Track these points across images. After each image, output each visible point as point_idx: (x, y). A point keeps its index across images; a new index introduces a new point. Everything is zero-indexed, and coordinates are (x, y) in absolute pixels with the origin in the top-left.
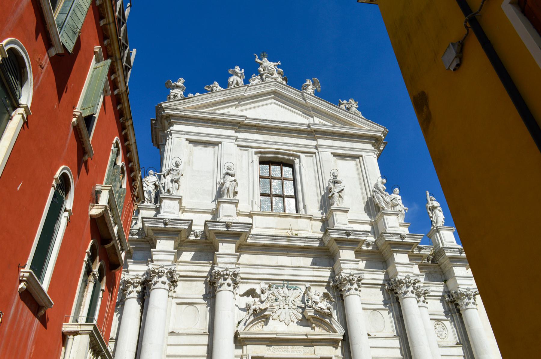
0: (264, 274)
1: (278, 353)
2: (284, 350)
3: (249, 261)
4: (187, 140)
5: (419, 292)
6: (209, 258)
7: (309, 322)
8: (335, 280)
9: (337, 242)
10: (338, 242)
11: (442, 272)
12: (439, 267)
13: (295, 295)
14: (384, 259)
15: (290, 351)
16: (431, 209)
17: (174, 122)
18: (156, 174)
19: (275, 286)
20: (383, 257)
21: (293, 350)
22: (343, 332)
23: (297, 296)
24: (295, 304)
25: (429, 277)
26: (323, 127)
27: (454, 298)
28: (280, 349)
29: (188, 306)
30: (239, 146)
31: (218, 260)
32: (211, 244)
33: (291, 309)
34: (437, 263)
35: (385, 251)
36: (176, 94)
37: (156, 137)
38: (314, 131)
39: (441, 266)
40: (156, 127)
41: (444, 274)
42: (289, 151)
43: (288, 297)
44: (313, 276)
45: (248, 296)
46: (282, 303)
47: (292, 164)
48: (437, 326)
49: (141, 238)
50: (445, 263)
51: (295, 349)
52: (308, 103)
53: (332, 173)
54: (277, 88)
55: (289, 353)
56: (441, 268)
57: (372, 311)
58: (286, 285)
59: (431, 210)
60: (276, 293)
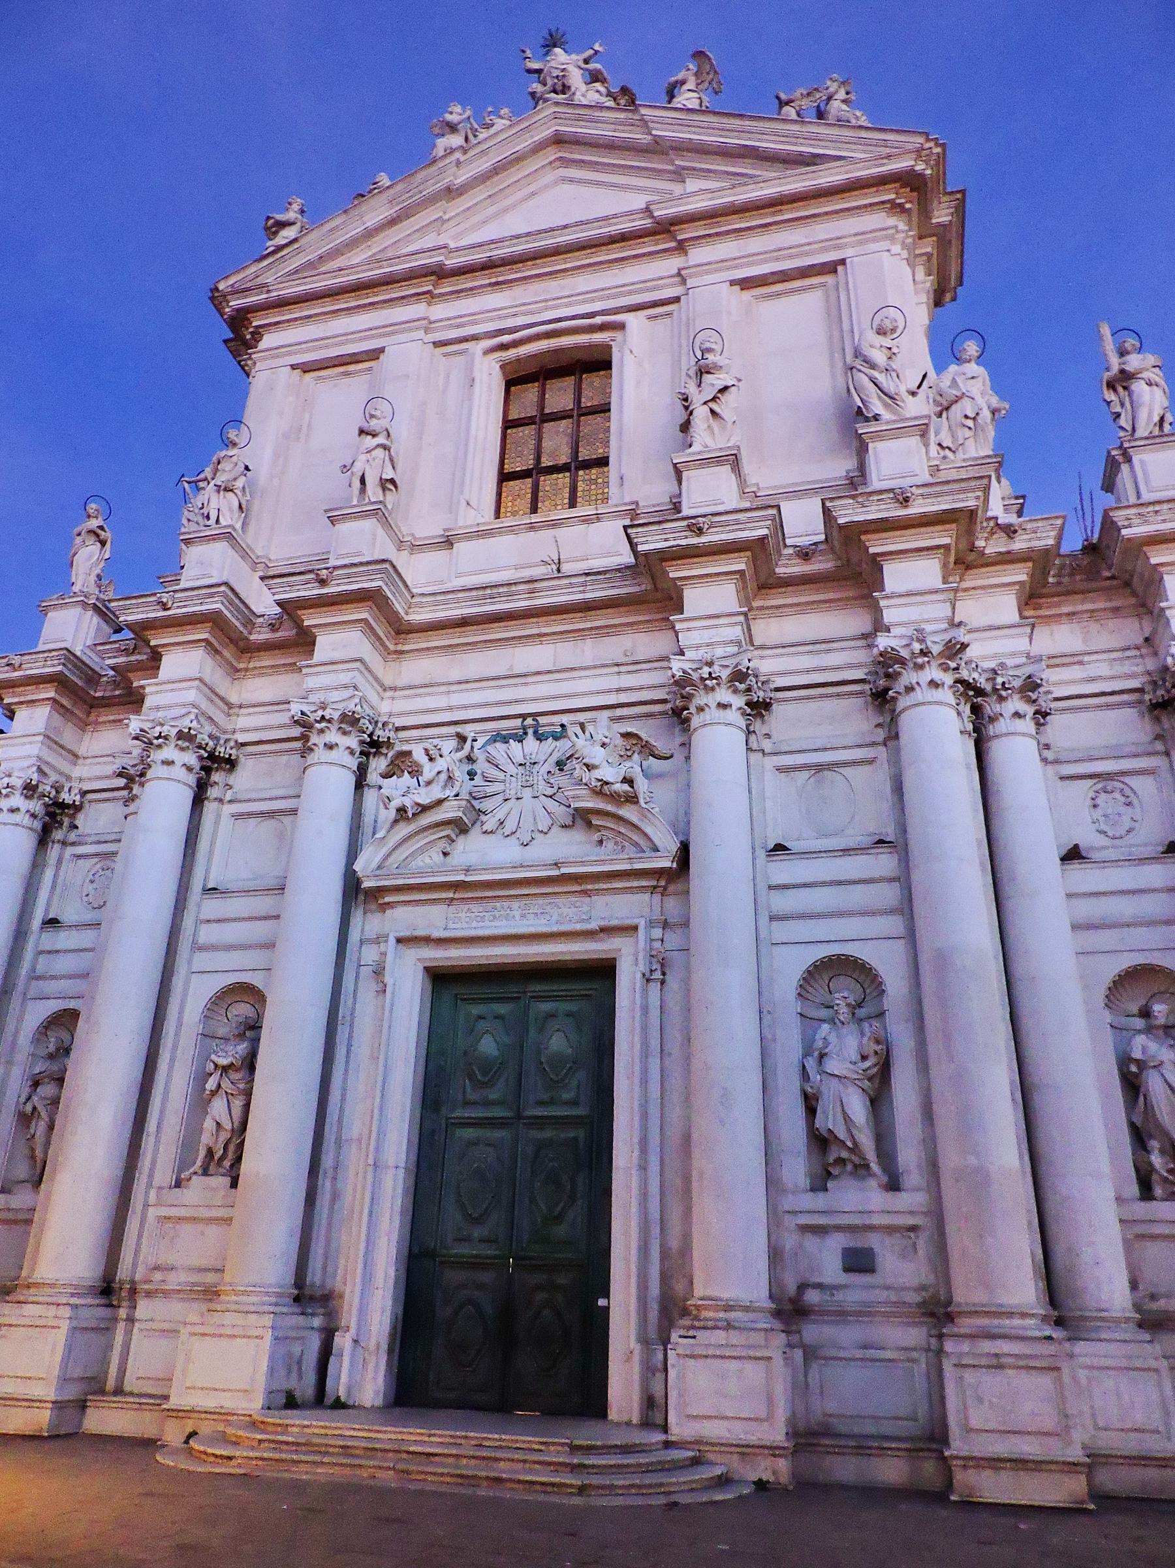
0: (465, 707)
1: (481, 924)
2: (496, 913)
5: (999, 687)
15: (517, 917)
21: (527, 912)
24: (552, 781)
26: (697, 202)
30: (438, 344)
34: (1113, 578)
43: (535, 763)
44: (619, 690)
47: (606, 358)
48: (1102, 799)
54: (560, 125)
55: (512, 923)
57: (813, 772)
58: (530, 731)
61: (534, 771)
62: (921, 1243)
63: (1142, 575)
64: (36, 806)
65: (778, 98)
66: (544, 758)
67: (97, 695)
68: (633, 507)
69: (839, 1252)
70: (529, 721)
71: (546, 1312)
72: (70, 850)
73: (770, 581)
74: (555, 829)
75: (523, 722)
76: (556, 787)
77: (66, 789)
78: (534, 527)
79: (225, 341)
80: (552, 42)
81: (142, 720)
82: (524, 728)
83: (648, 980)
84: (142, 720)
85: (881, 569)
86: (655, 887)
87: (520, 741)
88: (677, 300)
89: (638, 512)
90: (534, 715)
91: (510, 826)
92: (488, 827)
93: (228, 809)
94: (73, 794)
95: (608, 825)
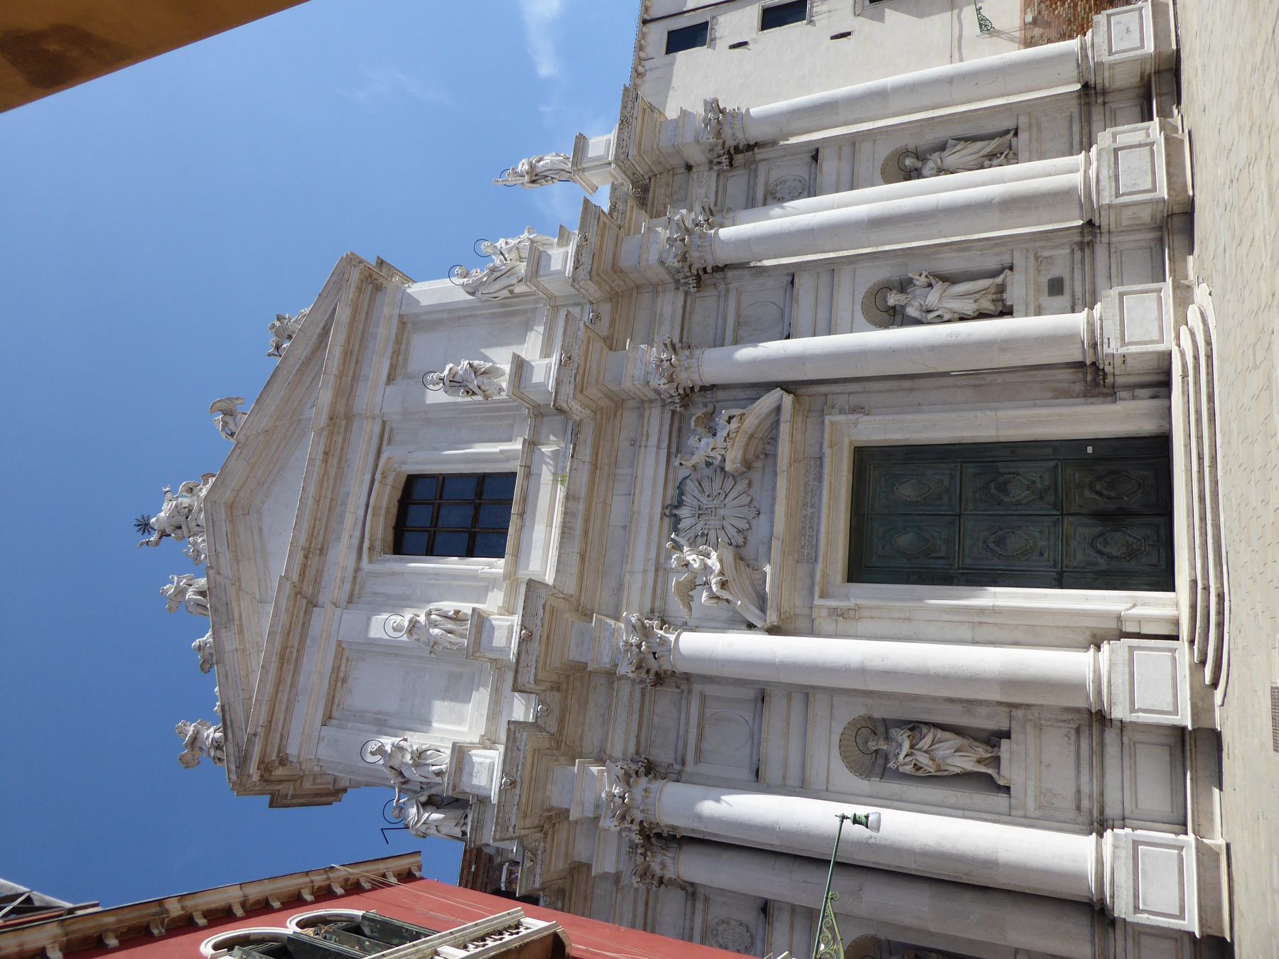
6: (601, 685)
7: (755, 465)
8: (670, 400)
11: (669, 171)
12: (658, 176)
13: (696, 491)
14: (632, 289)
16: (534, 178)
17: (279, 752)
18: (398, 801)
19: (672, 536)
22: (778, 392)
24: (715, 494)
31: (606, 664)
32: (571, 678)
34: (650, 179)
35: (613, 285)
36: (214, 743)
37: (316, 795)
40: (290, 794)
41: (673, 169)
46: (713, 522)
49: (545, 842)
50: (650, 163)
51: (809, 500)
58: (675, 512)
59: (536, 178)
60: (689, 536)
61: (705, 507)
62: (1047, 253)
65: (269, 355)
66: (696, 501)
69: (1050, 298)
70: (667, 512)
71: (1098, 487)
74: (751, 492)
79: (271, 805)
80: (145, 526)
85: (622, 271)
87: (680, 520)
88: (384, 423)
90: (664, 508)
91: (742, 525)
92: (740, 540)
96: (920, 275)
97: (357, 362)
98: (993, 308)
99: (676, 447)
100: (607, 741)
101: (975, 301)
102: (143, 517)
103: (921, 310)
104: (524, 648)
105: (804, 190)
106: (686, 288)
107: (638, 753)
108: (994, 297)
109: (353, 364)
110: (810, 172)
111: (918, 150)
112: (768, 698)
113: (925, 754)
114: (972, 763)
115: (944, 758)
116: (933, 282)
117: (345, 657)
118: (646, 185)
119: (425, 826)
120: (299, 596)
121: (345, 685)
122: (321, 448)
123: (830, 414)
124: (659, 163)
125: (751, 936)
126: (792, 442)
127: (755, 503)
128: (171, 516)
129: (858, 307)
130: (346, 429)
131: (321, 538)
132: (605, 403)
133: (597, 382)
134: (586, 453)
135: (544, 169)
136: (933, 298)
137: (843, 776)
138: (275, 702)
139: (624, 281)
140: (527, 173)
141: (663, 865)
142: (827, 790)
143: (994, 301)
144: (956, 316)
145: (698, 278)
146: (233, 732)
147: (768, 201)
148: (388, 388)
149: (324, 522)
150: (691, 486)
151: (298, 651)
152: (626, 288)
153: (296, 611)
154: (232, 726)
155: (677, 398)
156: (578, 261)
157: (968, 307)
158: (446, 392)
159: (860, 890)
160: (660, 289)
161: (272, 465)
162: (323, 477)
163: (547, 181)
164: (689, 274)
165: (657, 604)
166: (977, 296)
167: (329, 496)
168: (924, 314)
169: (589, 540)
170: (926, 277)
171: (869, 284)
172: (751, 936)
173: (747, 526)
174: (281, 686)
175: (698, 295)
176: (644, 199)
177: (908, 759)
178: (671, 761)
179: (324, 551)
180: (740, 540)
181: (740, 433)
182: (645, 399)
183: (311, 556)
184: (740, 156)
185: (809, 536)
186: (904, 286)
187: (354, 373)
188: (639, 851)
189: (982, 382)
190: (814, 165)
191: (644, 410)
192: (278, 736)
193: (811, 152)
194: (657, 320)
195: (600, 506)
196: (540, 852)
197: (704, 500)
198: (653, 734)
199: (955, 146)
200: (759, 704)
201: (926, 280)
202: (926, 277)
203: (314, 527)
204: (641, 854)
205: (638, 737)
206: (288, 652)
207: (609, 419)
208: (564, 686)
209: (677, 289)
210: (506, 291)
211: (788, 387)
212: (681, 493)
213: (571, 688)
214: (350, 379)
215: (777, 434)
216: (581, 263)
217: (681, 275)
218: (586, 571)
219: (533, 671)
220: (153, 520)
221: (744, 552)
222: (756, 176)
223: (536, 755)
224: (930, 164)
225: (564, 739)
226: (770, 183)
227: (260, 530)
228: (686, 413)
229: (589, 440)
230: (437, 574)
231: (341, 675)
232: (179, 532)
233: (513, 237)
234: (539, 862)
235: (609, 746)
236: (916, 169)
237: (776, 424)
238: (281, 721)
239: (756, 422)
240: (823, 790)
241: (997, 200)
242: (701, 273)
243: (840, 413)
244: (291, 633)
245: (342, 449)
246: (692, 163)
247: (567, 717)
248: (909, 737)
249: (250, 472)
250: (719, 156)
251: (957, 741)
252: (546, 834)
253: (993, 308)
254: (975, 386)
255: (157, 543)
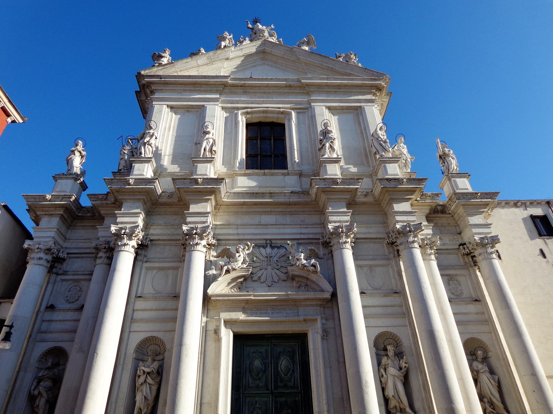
3: (228, 222)
4: (171, 108)
7: (294, 282)
8: (325, 236)
9: (325, 193)
10: (326, 193)
11: (457, 223)
12: (452, 218)
13: (280, 254)
14: (384, 211)
16: (443, 157)
17: (156, 90)
20: (382, 208)
21: (274, 311)
22: (331, 290)
23: (281, 256)
24: (278, 264)
25: (441, 230)
27: (470, 250)
28: (258, 312)
29: (159, 271)
32: (186, 206)
33: (275, 270)
34: (450, 214)
35: (383, 201)
37: (144, 110)
38: (306, 85)
39: (454, 217)
42: (279, 108)
45: (223, 257)
50: (458, 212)
51: (275, 311)
52: (300, 59)
53: (323, 124)
56: (454, 219)
57: (369, 267)
59: (443, 158)
60: (257, 254)
61: (271, 260)
63: (459, 214)
64: (49, 257)
65: (336, 54)
67: (79, 214)
68: (301, 172)
70: (268, 242)
72: (59, 277)
73: (353, 202)
75: (266, 241)
76: (280, 266)
77: (61, 252)
78: (273, 174)
79: (136, 92)
81: (104, 228)
82: (267, 243)
83: (323, 339)
84: (104, 228)
86: (322, 304)
88: (307, 109)
89: (302, 174)
90: (270, 240)
91: (263, 279)
92: (255, 279)
93: (146, 265)
94: (64, 254)
95: (303, 281)
96: (406, 363)
97: (336, 92)
98: (392, 407)
99: (300, 242)
100: (157, 226)
101: (393, 396)
102: (259, 20)
103: (385, 365)
104: (193, 181)
105: (457, 296)
106: (386, 237)
107: (151, 240)
108: (398, 407)
109: (335, 90)
110: (466, 298)
111: (487, 359)
112: (175, 299)
113: (144, 380)
114: (139, 406)
115: (141, 391)
116: (403, 371)
117: (198, 110)
118: (446, 212)
119: (122, 153)
120: (223, 86)
121: (186, 112)
122: (292, 83)
123: (322, 318)
124: (459, 217)
125: (73, 302)
126: (305, 300)
127: (275, 284)
128: (259, 30)
129: (385, 329)
130: (303, 93)
131: (251, 91)
132: (321, 204)
133: (328, 199)
134: (294, 199)
135: (448, 161)
136: (392, 371)
137: (135, 340)
138: (177, 84)
139: (386, 206)
140: (444, 153)
141: (101, 257)
142: (130, 332)
143: (396, 407)
144: (384, 385)
145: (393, 243)
146: (162, 69)
147: (446, 277)
148: (324, 107)
149: (258, 91)
150: (282, 251)
151: (199, 90)
152: (384, 208)
153: (216, 86)
154: (165, 68)
155: (325, 239)
156: (391, 180)
157: (390, 392)
158: (320, 131)
159: (82, 352)
160: (385, 225)
161: (285, 65)
162: (279, 87)
163: (442, 164)
164: (393, 238)
165: (223, 242)
166: (397, 397)
167: (271, 91)
168: (383, 367)
169: (252, 206)
170: (405, 367)
171: (399, 335)
172: (73, 302)
173: (262, 281)
174: (183, 85)
175: (385, 244)
176: (438, 212)
177: (142, 372)
178: (148, 256)
179: (245, 93)
180: (255, 279)
181: (307, 272)
182: (325, 224)
183: (242, 88)
184: (470, 259)
185: (257, 313)
186: (399, 355)
187: (330, 91)
188: (106, 246)
189: (345, 402)
190: (471, 299)
191: (320, 224)
192: (161, 88)
193: (478, 298)
194: (368, 225)
195: (270, 210)
196: (106, 202)
197: (275, 259)
198: (161, 247)
199: (494, 380)
200: (174, 295)
201: (404, 367)
202: (405, 367)
203: (255, 87)
204: (105, 247)
205: (159, 240)
206: (198, 86)
207: (314, 208)
208: (182, 203)
209: (386, 234)
210: (375, 150)
211: (334, 295)
212: (278, 248)
213: (181, 207)
214: (327, 90)
215: (310, 291)
216: (390, 182)
217: (392, 234)
218: (237, 207)
219: (182, 186)
220: (258, 24)
221: (249, 281)
222: (460, 269)
223: (145, 193)
224: (480, 366)
225: (158, 206)
226: (458, 277)
227: (254, 66)
228: (321, 245)
229: (300, 200)
230: (236, 142)
231: (190, 110)
232: (253, 34)
233: (409, 152)
234: (102, 202)
235: (155, 227)
236: (477, 358)
237: (314, 290)
238: (169, 88)
239: (315, 280)
240: (130, 329)
241: (454, 406)
242: (396, 244)
243: (323, 324)
244: (206, 86)
245: (294, 93)
246: (463, 234)
247: (167, 207)
248: (153, 371)
249: (280, 57)
250: (468, 248)
251: (151, 398)
252: (114, 203)
253: (392, 407)
254: (343, 398)
255: (249, 28)
